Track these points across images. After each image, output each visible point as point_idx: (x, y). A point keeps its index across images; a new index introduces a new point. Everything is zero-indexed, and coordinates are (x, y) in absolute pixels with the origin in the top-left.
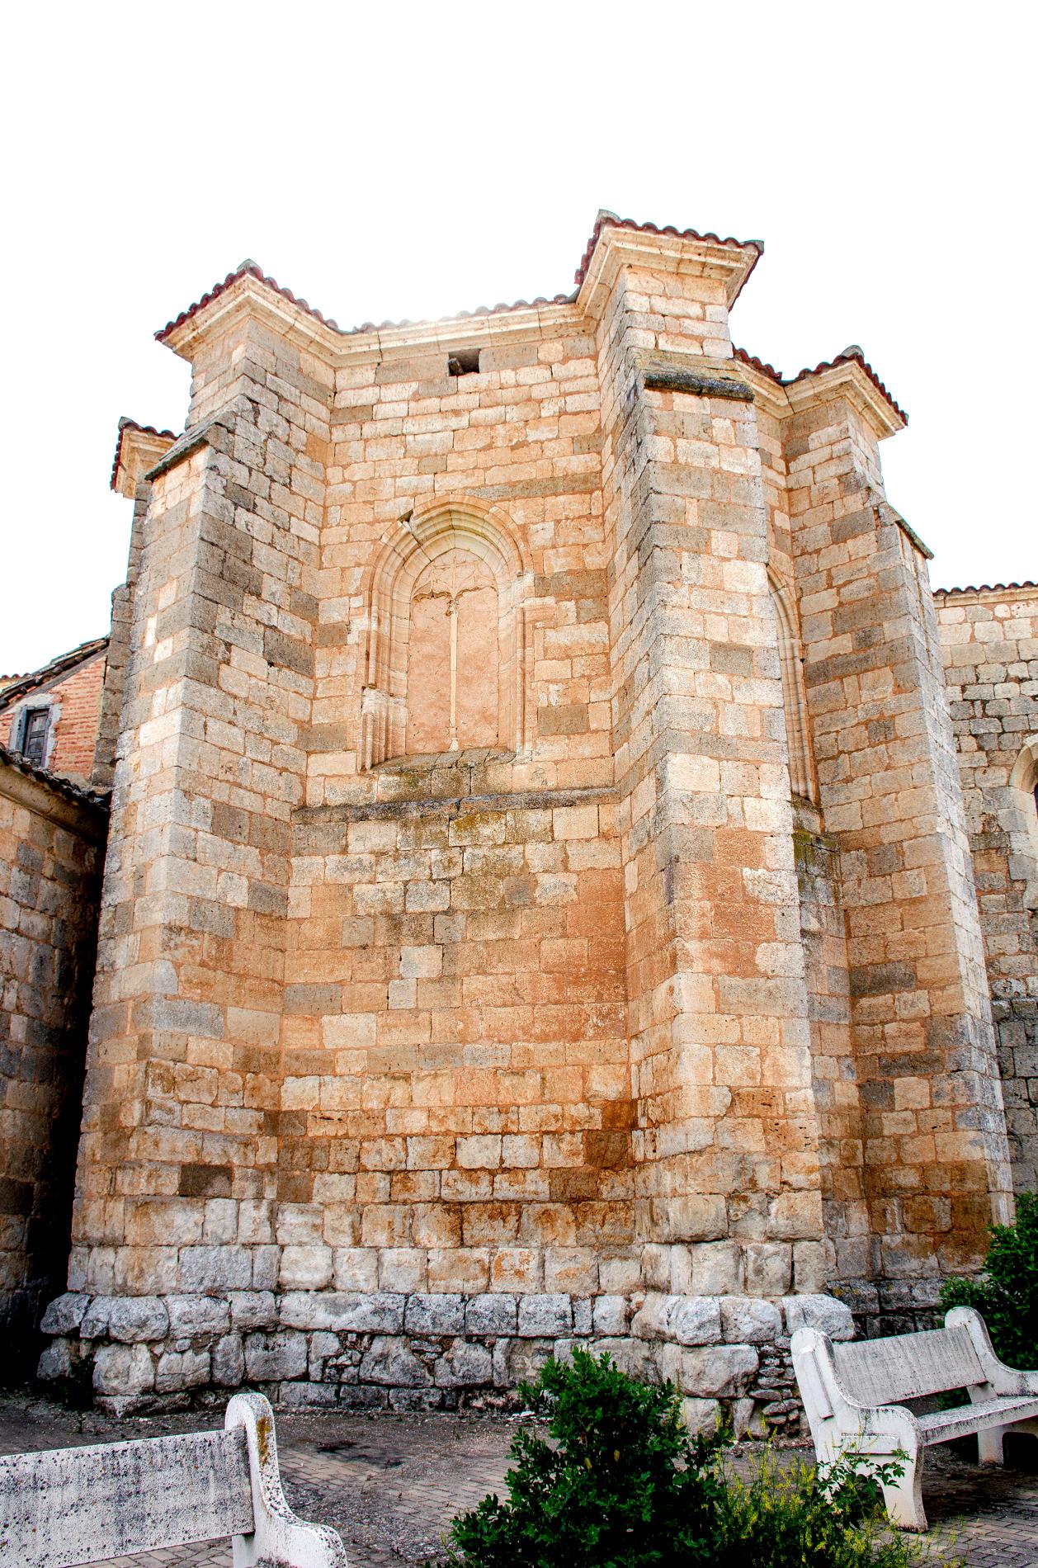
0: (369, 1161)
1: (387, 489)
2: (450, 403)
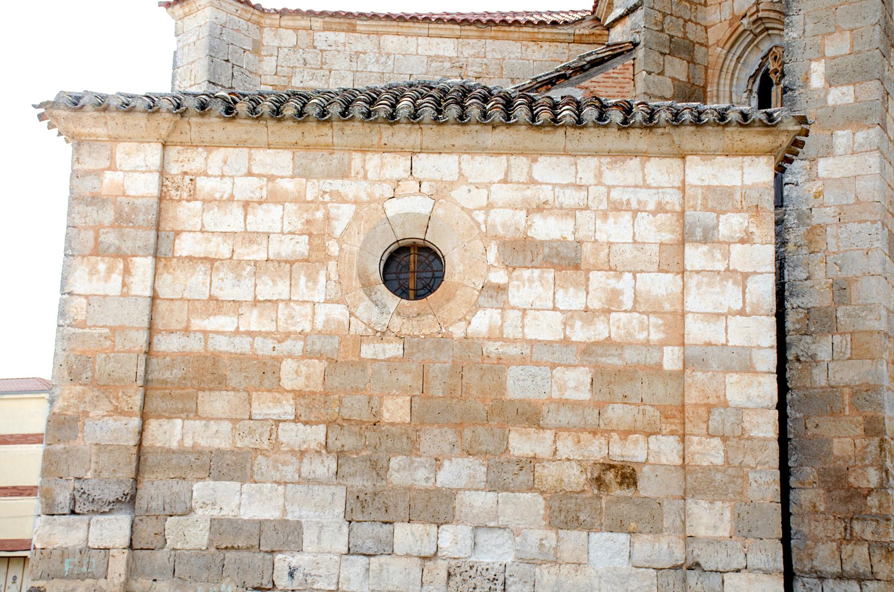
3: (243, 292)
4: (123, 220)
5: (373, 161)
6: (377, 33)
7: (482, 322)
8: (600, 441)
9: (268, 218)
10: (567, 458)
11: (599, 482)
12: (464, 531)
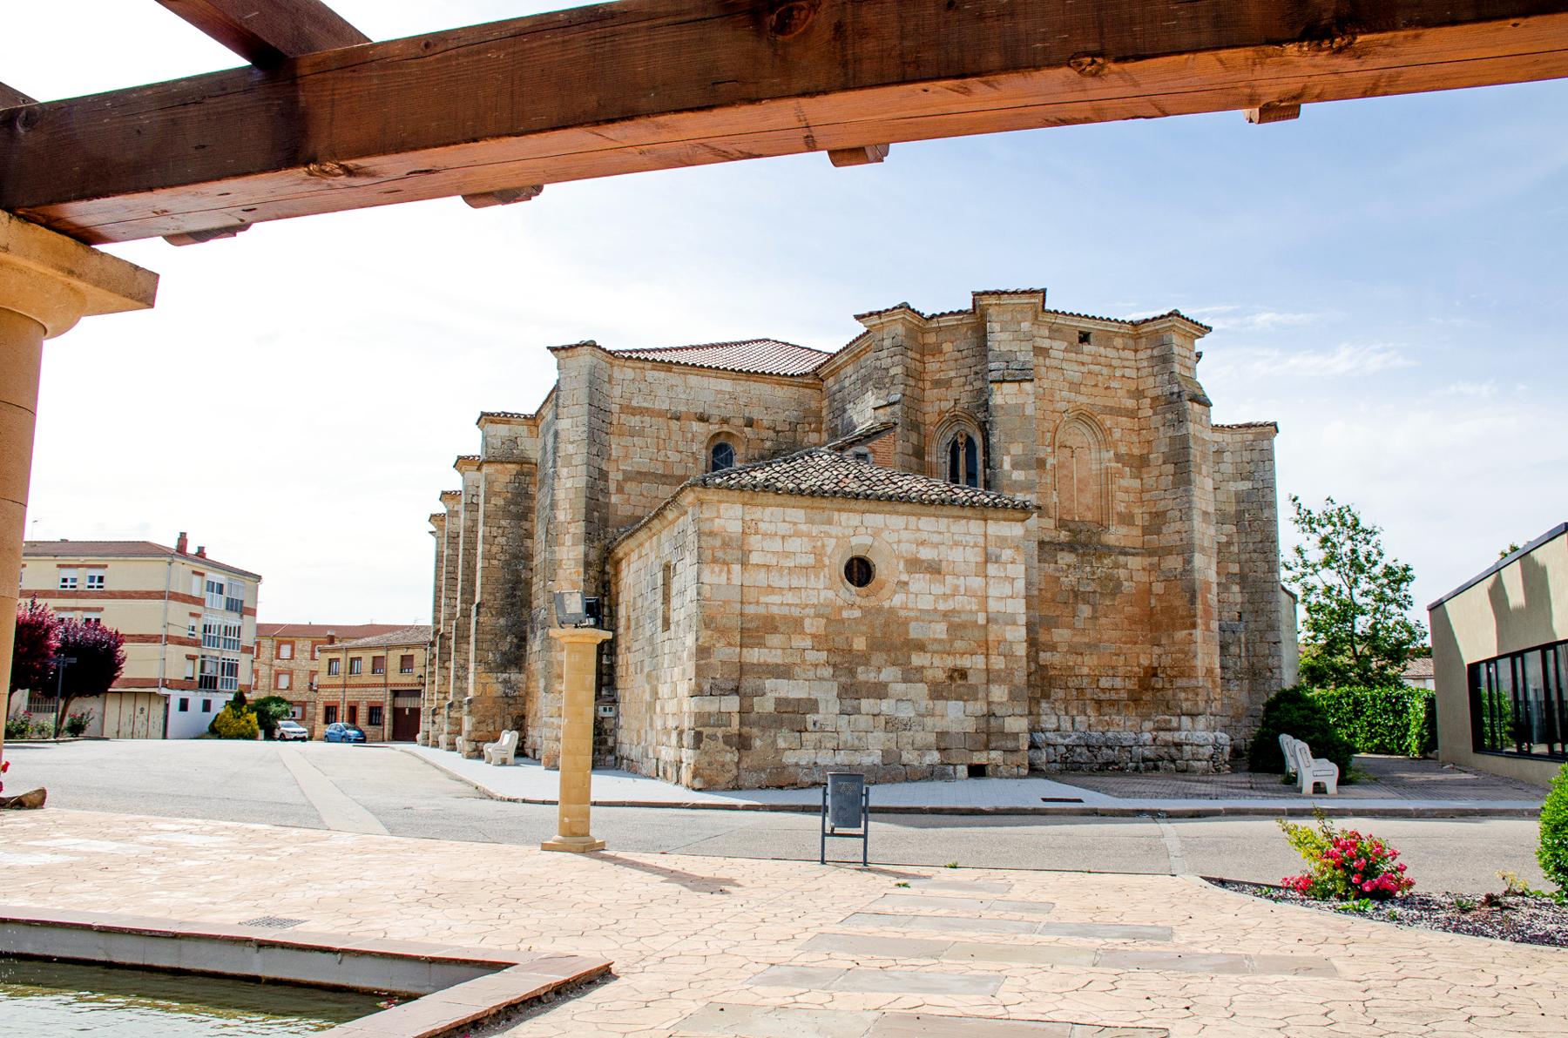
0: (1070, 684)
1: (1057, 397)
2: (1080, 358)
3: (784, 583)
4: (725, 545)
5: (844, 516)
7: (898, 600)
8: (951, 658)
9: (794, 545)
10: (935, 665)
11: (951, 677)
12: (892, 702)
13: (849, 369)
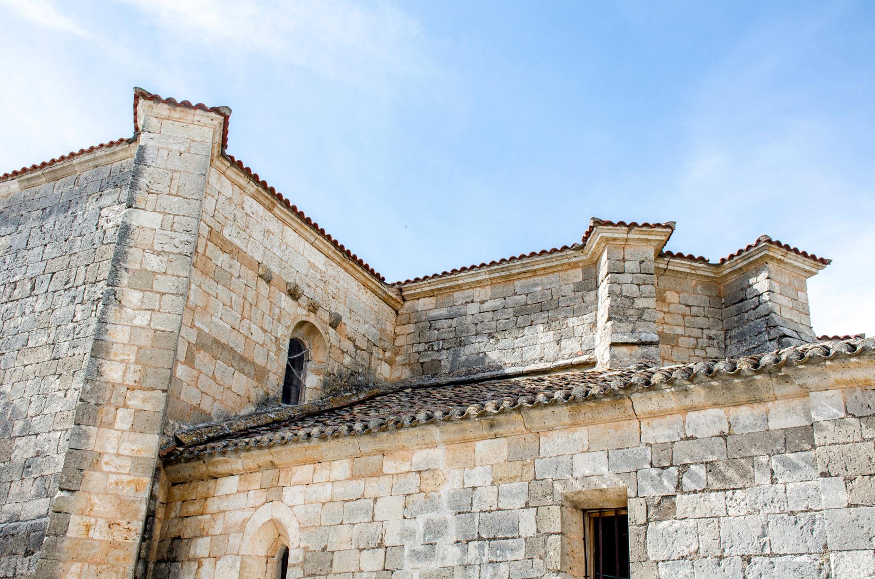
6: (284, 222)
13: (479, 293)
